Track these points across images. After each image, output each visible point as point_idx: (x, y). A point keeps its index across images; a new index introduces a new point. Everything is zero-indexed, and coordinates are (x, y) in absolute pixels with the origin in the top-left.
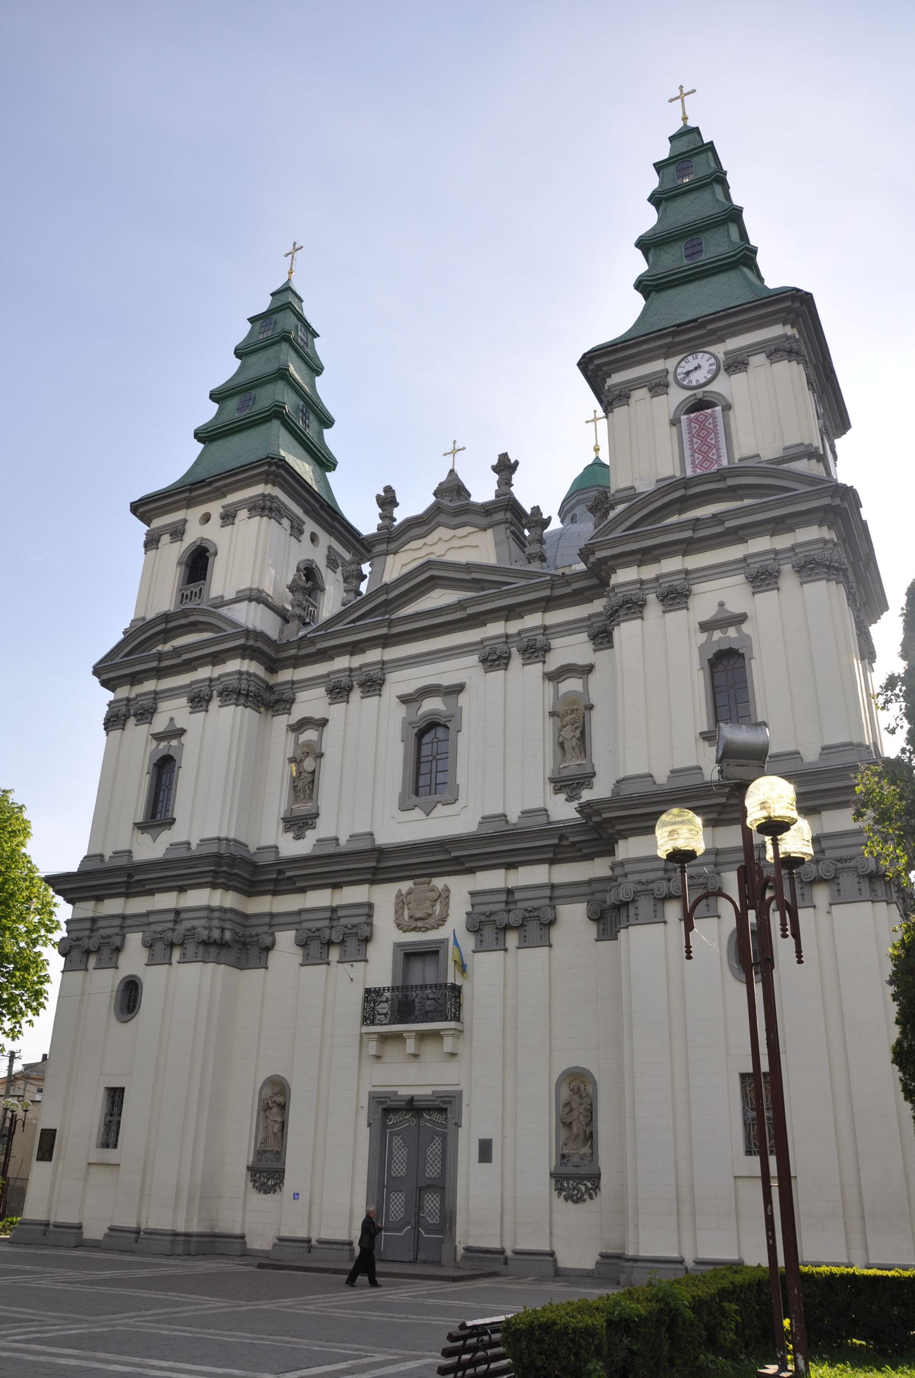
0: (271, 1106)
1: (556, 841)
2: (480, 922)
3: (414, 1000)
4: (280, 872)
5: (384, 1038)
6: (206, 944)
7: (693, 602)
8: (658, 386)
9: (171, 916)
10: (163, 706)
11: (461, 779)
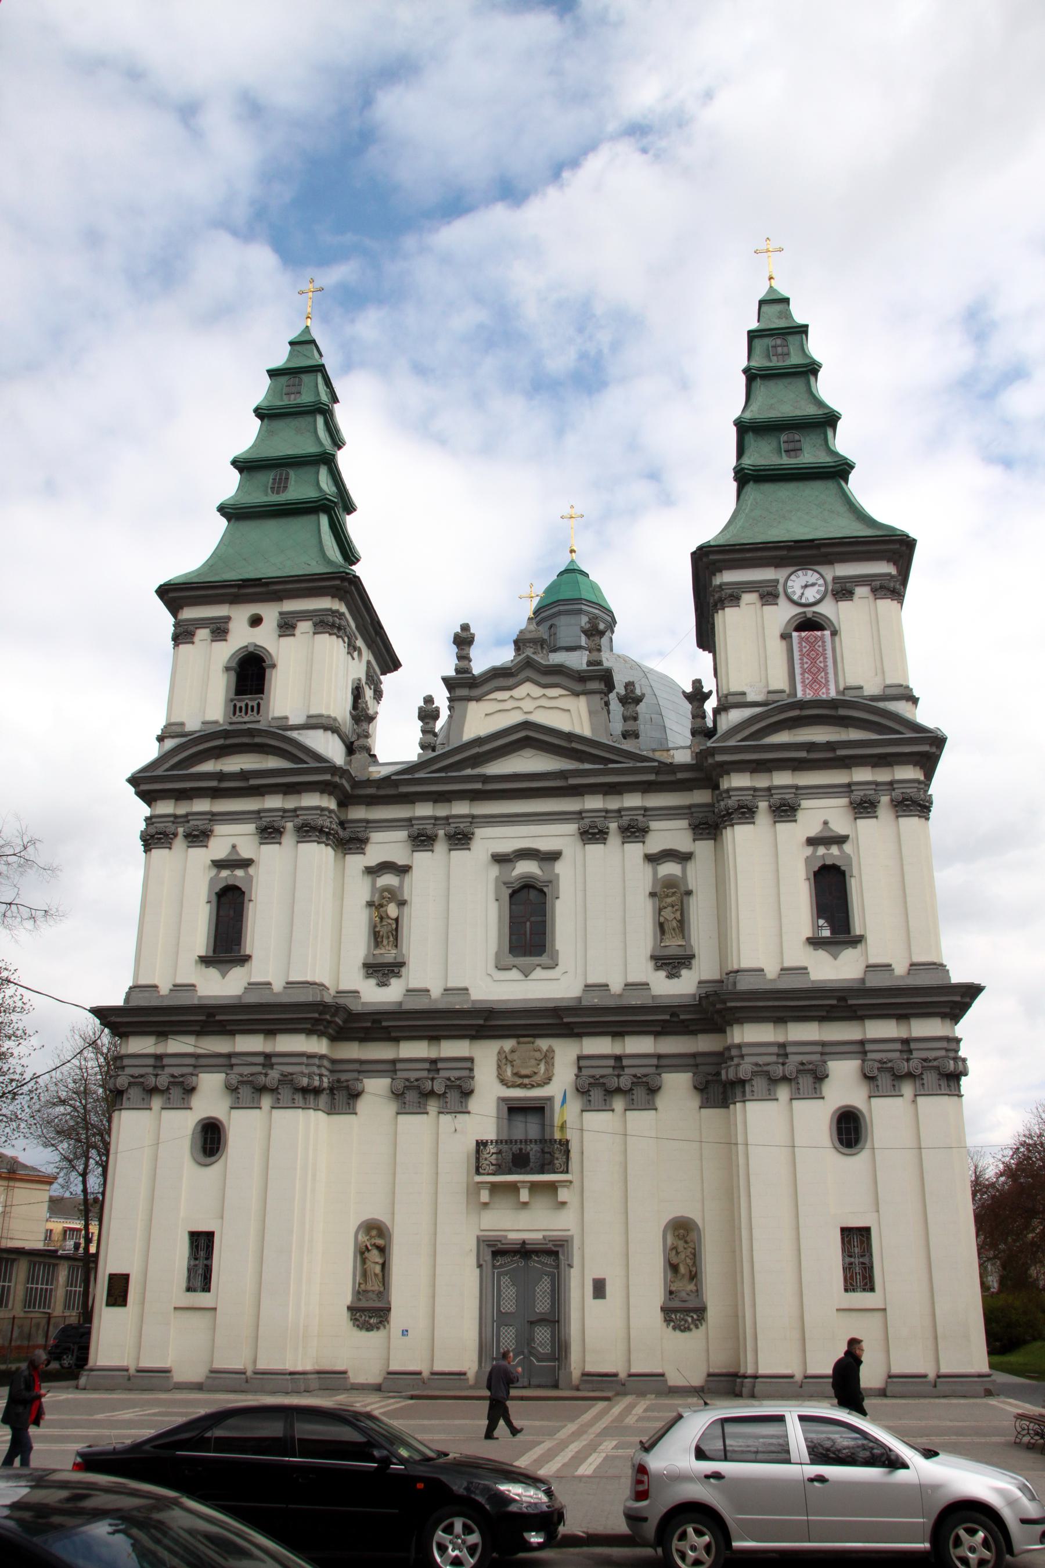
0: (370, 1248)
1: (667, 1017)
2: (589, 1084)
3: (528, 1153)
4: (374, 1021)
5: (494, 1188)
7: (800, 815)
8: (769, 595)
9: (260, 1060)
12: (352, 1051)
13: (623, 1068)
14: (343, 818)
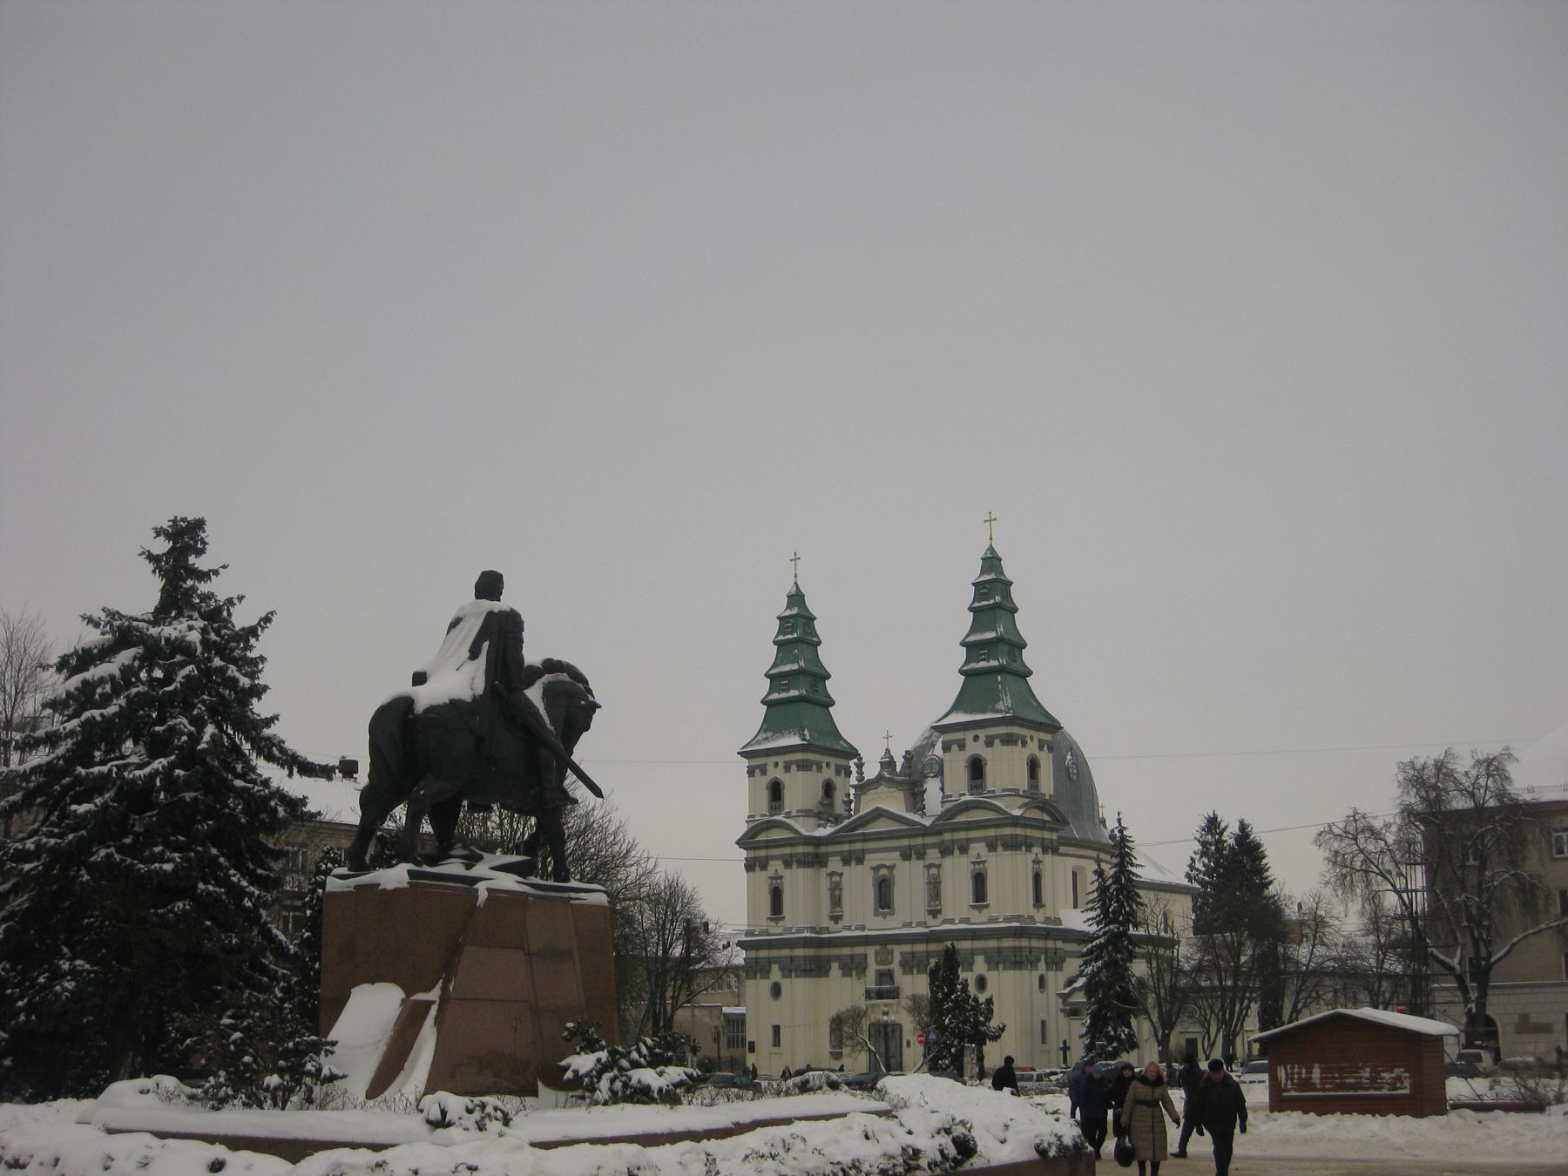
5: (873, 1005)
6: (805, 970)
10: (771, 863)
11: (896, 906)
12: (825, 952)
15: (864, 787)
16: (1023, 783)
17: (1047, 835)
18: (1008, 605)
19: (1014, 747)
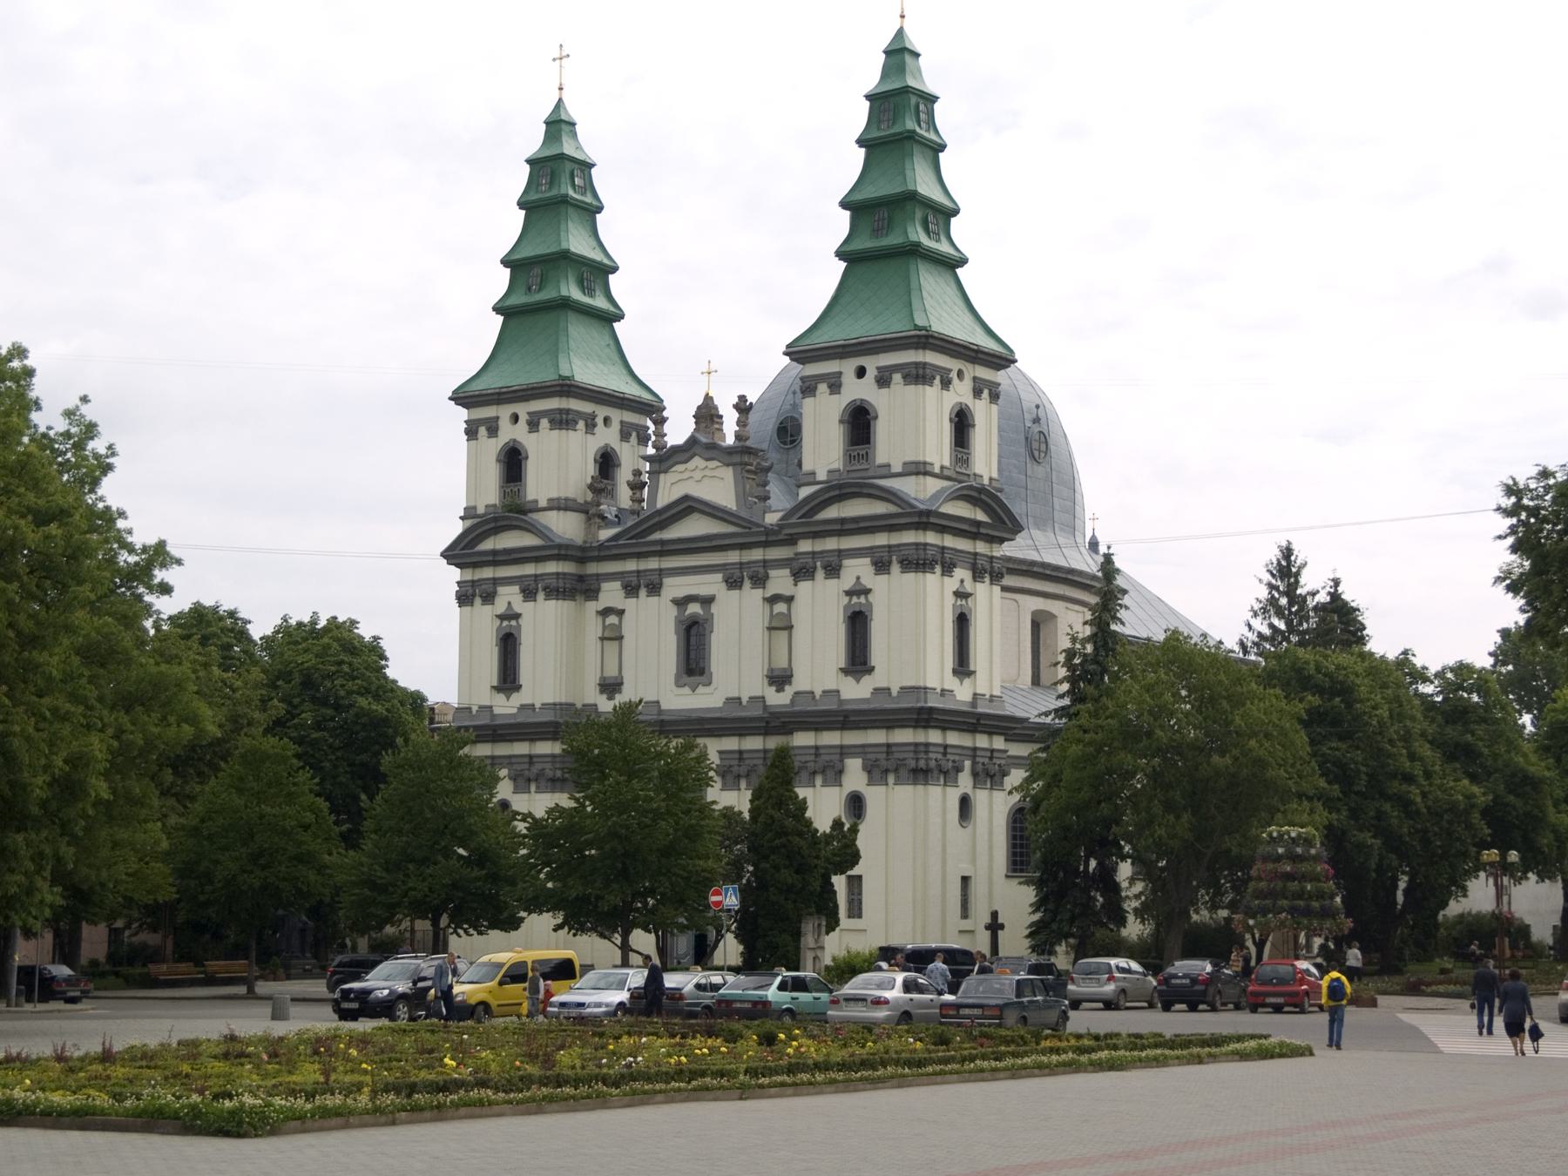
6: (553, 780)
7: (843, 572)
8: (835, 385)
9: (527, 760)
10: (501, 590)
11: (713, 669)
13: (744, 759)
14: (581, 573)
15: (667, 458)
16: (938, 451)
17: (981, 547)
18: (926, 134)
19: (927, 387)
